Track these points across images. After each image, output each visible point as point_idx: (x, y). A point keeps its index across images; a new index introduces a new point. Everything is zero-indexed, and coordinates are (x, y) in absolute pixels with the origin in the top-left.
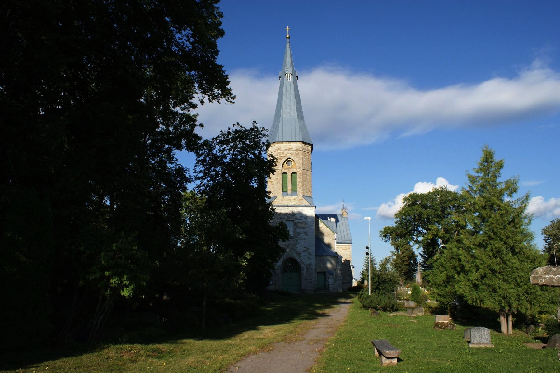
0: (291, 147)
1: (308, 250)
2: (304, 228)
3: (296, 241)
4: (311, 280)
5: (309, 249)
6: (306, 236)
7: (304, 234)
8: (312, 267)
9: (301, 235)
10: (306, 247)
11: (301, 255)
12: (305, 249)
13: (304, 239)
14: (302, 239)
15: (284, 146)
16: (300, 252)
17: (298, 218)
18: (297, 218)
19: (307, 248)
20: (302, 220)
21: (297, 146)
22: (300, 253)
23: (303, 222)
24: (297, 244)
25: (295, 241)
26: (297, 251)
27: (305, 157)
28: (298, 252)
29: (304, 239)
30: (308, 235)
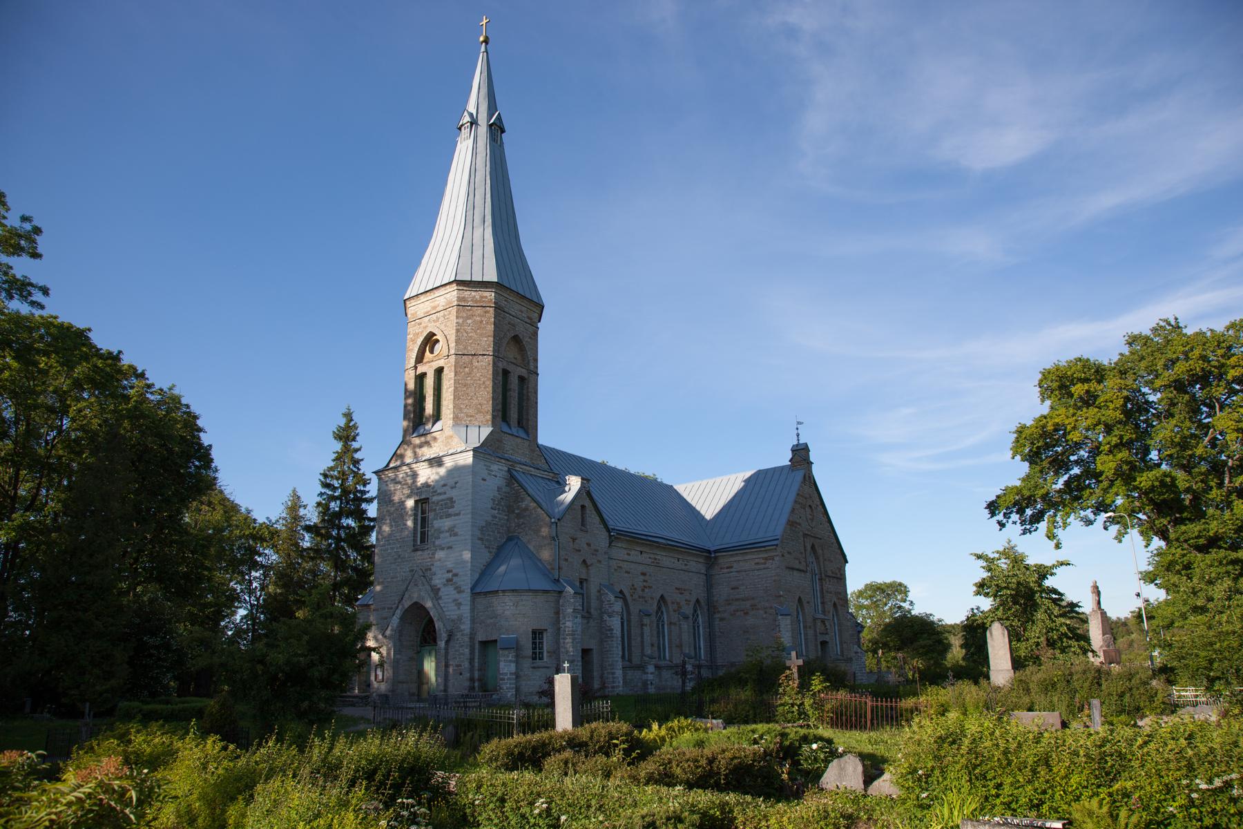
0: (433, 304)
1: (455, 579)
2: (449, 516)
5: (456, 575)
6: (453, 538)
7: (448, 534)
8: (462, 627)
9: (442, 535)
11: (440, 594)
12: (450, 575)
15: (422, 305)
17: (439, 491)
18: (435, 492)
19: (454, 571)
20: (445, 493)
21: (448, 296)
22: (439, 589)
23: (448, 499)
27: (469, 321)
30: (456, 535)
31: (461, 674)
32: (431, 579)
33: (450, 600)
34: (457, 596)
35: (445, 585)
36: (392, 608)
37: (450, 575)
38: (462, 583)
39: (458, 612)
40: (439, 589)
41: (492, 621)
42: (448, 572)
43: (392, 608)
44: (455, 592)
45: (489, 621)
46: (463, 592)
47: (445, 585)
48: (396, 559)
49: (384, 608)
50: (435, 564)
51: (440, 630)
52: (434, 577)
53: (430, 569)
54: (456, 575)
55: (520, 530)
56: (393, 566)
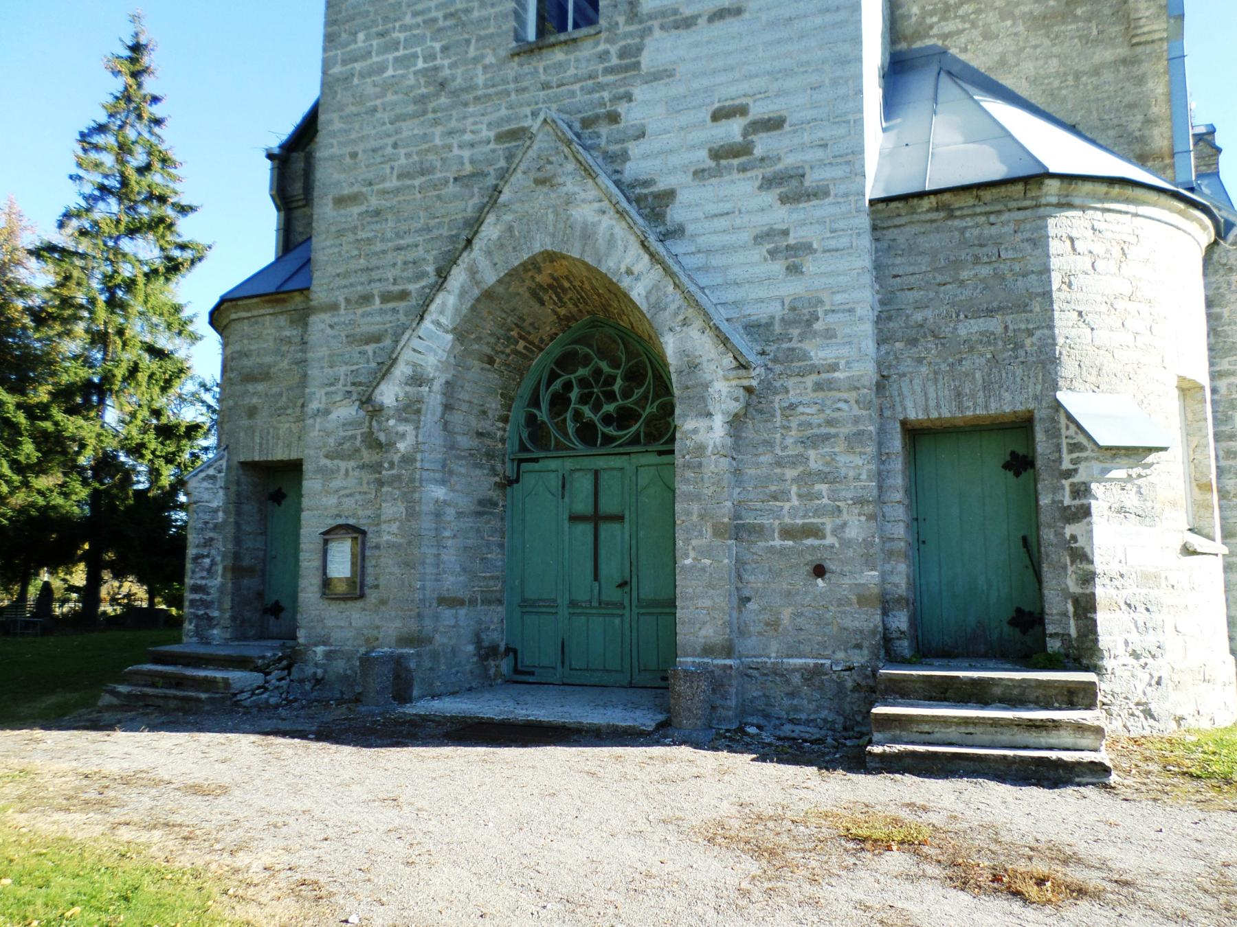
1: (763, 144)
3: (623, 54)
4: (816, 532)
5: (773, 124)
8: (819, 353)
10: (742, 111)
11: (676, 214)
12: (733, 130)
13: (720, 14)
14: (688, 23)
16: (661, 186)
19: (758, 110)
22: (669, 196)
24: (629, 97)
25: (615, 61)
26: (632, 169)
28: (632, 186)
29: (720, 14)
31: (819, 571)
32: (624, 156)
33: (745, 237)
34: (780, 215)
35: (699, 174)
36: (404, 295)
37: (733, 130)
38: (810, 156)
39: (794, 288)
40: (669, 196)
41: (994, 324)
42: (717, 116)
43: (404, 295)
44: (771, 197)
45: (970, 328)
46: (819, 193)
47: (699, 174)
48: (422, 100)
49: (366, 299)
50: (638, 92)
51: (693, 367)
52: (634, 149)
53: (614, 118)
54: (773, 124)
55: (949, 27)
56: (410, 129)
